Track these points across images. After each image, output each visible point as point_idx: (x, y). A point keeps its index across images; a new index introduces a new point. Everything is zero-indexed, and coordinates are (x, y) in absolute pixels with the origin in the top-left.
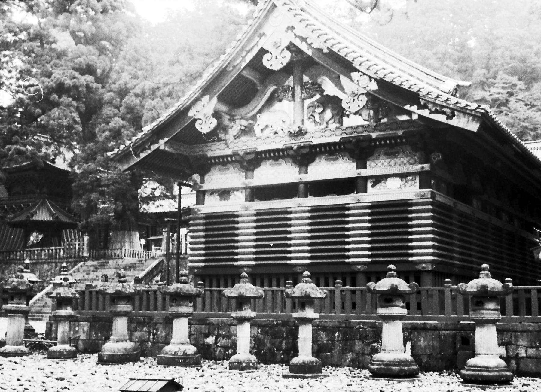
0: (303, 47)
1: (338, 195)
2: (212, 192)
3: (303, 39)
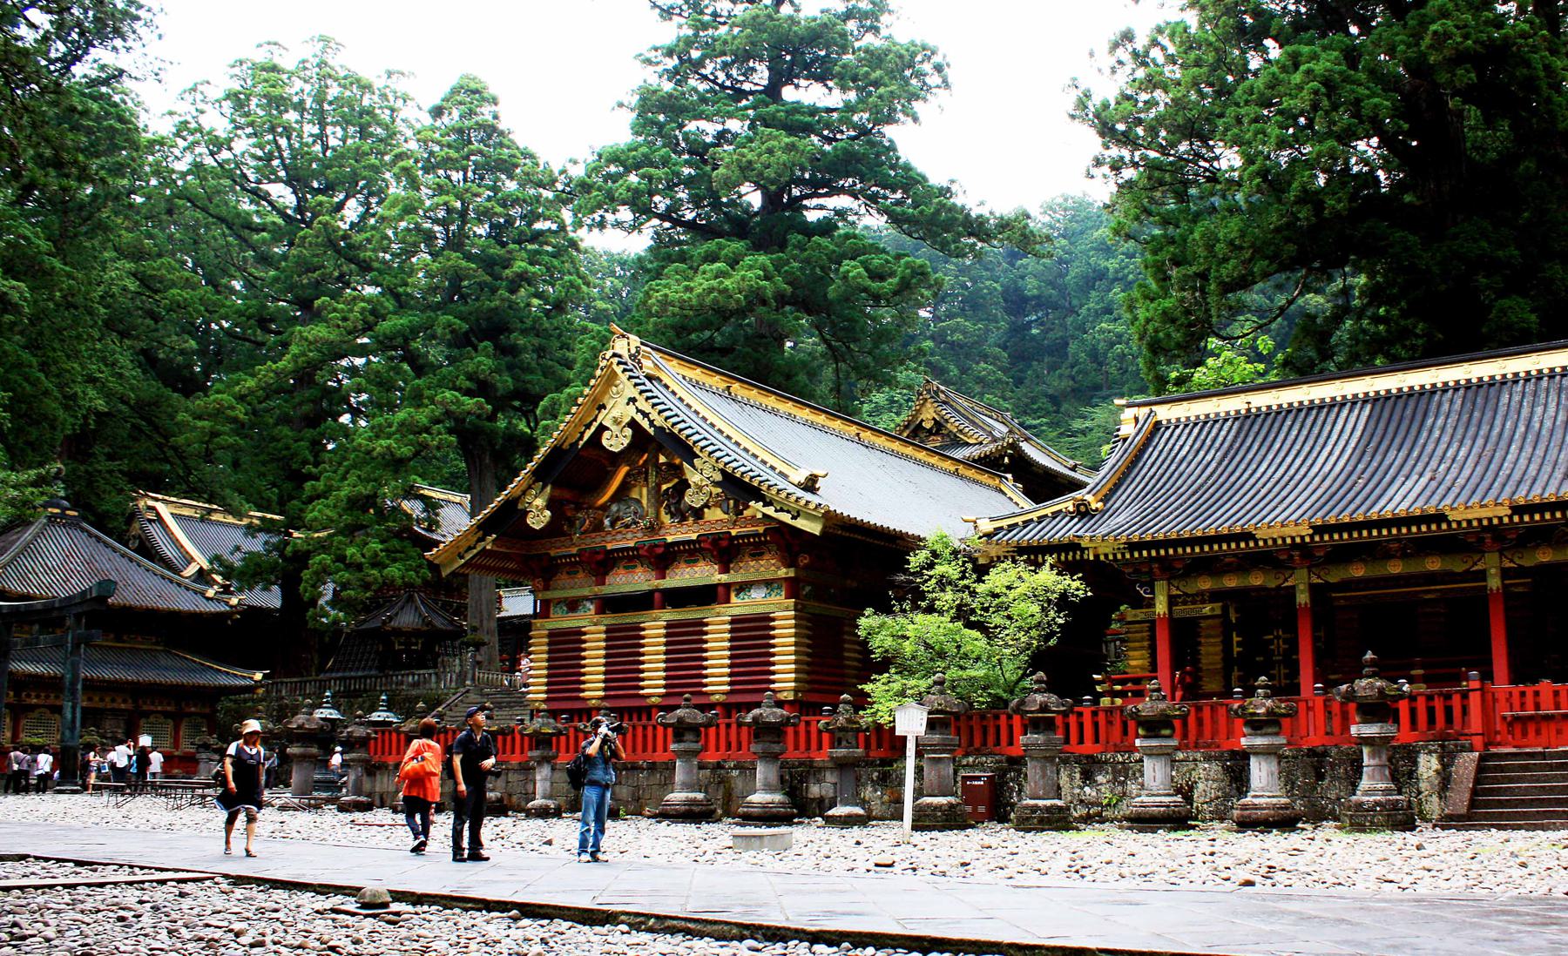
0: (645, 424)
1: (699, 605)
2: (559, 602)
3: (645, 415)
